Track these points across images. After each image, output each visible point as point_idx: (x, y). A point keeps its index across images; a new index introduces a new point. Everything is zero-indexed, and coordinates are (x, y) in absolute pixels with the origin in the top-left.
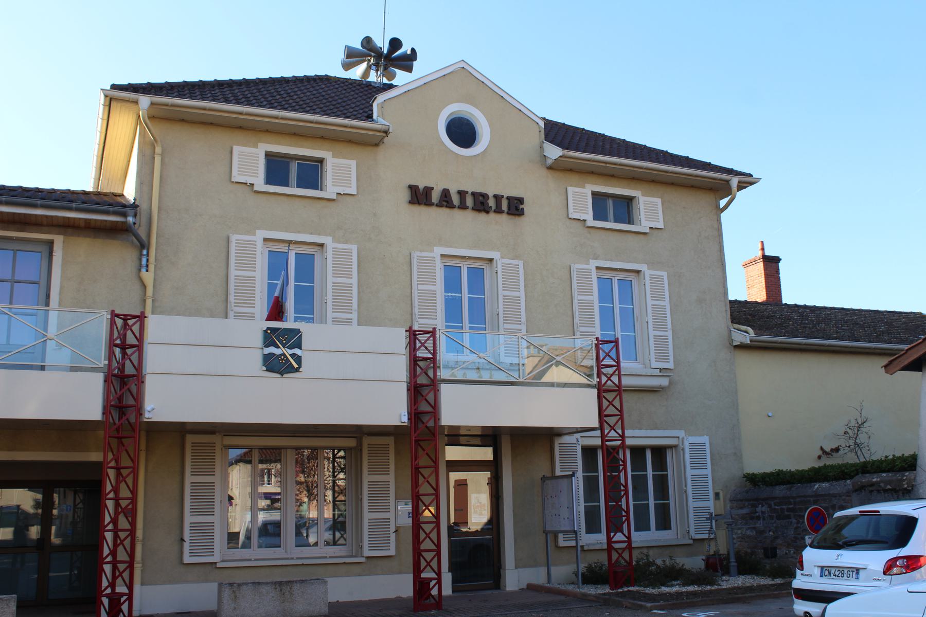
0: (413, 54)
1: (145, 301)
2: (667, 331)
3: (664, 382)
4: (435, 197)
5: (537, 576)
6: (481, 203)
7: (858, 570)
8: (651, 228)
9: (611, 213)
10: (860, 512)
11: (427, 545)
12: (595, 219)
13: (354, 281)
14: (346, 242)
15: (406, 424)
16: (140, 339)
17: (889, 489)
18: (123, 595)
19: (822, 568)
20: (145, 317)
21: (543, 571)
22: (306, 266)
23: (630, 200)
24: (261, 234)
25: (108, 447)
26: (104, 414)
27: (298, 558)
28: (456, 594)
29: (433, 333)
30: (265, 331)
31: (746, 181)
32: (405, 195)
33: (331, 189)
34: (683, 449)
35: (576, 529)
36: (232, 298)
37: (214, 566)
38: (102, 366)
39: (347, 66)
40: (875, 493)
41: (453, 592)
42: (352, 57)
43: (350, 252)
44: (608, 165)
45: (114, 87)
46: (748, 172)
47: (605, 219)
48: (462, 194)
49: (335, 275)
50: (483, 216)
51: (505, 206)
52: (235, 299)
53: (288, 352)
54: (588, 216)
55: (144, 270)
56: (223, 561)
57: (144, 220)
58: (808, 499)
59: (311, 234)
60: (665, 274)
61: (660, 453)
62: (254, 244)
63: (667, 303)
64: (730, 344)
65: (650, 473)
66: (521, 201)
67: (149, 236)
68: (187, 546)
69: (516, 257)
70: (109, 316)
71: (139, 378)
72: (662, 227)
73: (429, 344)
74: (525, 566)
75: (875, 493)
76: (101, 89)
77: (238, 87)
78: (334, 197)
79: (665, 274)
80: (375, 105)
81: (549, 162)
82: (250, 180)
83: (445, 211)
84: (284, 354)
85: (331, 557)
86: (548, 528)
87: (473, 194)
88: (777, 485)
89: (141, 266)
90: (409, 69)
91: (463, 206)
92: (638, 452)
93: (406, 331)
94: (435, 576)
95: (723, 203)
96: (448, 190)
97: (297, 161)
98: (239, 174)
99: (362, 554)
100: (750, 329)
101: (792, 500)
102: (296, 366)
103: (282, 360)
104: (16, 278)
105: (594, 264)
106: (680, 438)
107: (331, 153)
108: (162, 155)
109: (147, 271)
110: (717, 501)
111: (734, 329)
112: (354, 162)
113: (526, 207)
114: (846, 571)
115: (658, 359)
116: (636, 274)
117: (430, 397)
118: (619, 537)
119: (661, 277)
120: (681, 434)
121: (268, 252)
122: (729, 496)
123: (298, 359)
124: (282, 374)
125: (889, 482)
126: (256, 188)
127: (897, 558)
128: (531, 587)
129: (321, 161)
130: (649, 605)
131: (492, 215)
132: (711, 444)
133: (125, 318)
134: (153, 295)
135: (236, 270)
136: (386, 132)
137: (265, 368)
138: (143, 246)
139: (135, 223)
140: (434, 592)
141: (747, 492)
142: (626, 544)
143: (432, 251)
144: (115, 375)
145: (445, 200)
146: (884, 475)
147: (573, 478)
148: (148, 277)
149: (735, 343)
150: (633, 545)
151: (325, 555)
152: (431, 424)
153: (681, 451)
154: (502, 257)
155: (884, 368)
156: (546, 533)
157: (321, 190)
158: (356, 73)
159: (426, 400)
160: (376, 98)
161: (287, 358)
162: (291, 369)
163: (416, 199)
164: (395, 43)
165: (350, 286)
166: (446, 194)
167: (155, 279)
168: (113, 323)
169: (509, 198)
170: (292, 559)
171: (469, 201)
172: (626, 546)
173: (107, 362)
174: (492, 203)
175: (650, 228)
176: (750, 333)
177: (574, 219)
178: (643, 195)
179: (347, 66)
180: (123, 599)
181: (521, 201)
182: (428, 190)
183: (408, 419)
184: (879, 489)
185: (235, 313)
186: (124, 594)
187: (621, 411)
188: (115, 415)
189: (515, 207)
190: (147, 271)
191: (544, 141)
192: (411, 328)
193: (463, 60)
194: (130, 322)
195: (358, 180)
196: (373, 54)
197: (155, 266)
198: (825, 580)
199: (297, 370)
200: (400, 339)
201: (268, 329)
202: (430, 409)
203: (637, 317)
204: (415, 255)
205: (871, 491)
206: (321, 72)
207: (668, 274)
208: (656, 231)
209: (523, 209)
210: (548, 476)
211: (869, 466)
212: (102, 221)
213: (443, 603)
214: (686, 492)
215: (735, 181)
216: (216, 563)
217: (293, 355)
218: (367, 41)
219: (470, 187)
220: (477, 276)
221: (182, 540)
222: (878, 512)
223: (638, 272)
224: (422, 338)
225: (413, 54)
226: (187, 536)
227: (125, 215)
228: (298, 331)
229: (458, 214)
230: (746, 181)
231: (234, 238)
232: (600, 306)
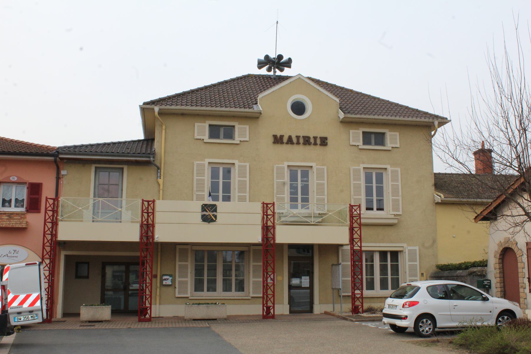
0: (290, 60)
1: (159, 191)
2: (399, 197)
3: (395, 221)
4: (285, 140)
5: (329, 308)
6: (307, 141)
7: (396, 306)
8: (393, 147)
9: (373, 141)
10: (407, 284)
11: (269, 292)
12: (364, 144)
13: (247, 179)
14: (244, 162)
15: (261, 242)
16: (153, 210)
17: (479, 275)
18: (148, 307)
19: (389, 305)
20: (155, 201)
21: (331, 306)
22: (228, 173)
23: (383, 134)
24: (207, 161)
25: (142, 251)
26: (140, 239)
27: (223, 296)
28: (291, 314)
29: (273, 204)
30: (202, 206)
31: (443, 121)
32: (272, 140)
33: (237, 139)
34: (405, 252)
35: (340, 288)
36: (195, 189)
37: (188, 298)
38: (139, 220)
39: (260, 67)
40: (475, 276)
41: (290, 313)
42: (261, 64)
43: (245, 166)
44: (368, 120)
45: (145, 104)
46: (445, 116)
47: (369, 143)
48: (298, 137)
49: (239, 177)
50: (307, 147)
51: (318, 141)
52: (196, 189)
53: (211, 214)
54: (360, 143)
55: (159, 178)
56: (192, 296)
57: (158, 157)
58: (454, 278)
59: (229, 159)
60: (399, 169)
61: (395, 255)
62: (204, 165)
63: (399, 183)
64: (433, 202)
65: (389, 263)
66: (326, 138)
67: (161, 164)
68: (177, 290)
69: (323, 165)
70: (141, 201)
71: (153, 226)
72: (399, 146)
73: (272, 208)
74: (324, 303)
75: (475, 276)
76: (139, 105)
77: (201, 91)
78: (239, 142)
79: (399, 169)
80: (258, 98)
81: (341, 120)
82: (202, 137)
83: (289, 146)
84: (210, 215)
85: (236, 296)
86: (334, 287)
87: (303, 137)
88: (446, 270)
89: (158, 176)
90: (290, 67)
91: (298, 143)
92: (383, 254)
93: (262, 203)
94: (272, 305)
95: (433, 133)
96: (291, 136)
97: (223, 127)
98: (197, 135)
99: (250, 296)
100: (442, 195)
101: (449, 278)
102: (214, 219)
103: (209, 217)
104: (111, 183)
105: (362, 166)
106: (404, 247)
107: (238, 123)
108: (166, 129)
109: (160, 178)
110: (422, 277)
111: (436, 194)
112: (248, 126)
113: (329, 141)
114: (394, 306)
115: (393, 210)
116: (384, 170)
117: (272, 231)
118: (357, 292)
119: (397, 171)
120: (405, 245)
121: (211, 168)
122: (429, 275)
123: (215, 217)
124: (209, 222)
125: (479, 272)
126: (205, 141)
127: (407, 302)
128: (326, 313)
129: (234, 126)
130: (354, 320)
131: (312, 147)
132: (419, 250)
133: (148, 202)
134: (163, 188)
135: (197, 176)
136: (261, 113)
137: (202, 220)
138: (159, 168)
139: (154, 161)
140: (272, 311)
141: (435, 273)
142: (360, 295)
143: (283, 164)
144: (144, 224)
145: (290, 141)
146: (479, 268)
147: (340, 265)
148: (161, 181)
149: (436, 202)
150: (364, 296)
151: (234, 295)
152: (272, 242)
153: (404, 254)
154: (317, 165)
155: (474, 220)
156: (333, 289)
157: (234, 140)
158: (264, 71)
159: (271, 232)
160: (258, 96)
161: (211, 216)
162: (212, 221)
163: (276, 141)
164: (280, 57)
165: (246, 181)
166: (290, 138)
167: (163, 182)
168: (143, 203)
169: (321, 138)
170: (220, 296)
171: (301, 141)
172: (361, 296)
173: (141, 219)
174: (312, 141)
175: (392, 147)
176: (442, 197)
177: (353, 145)
178: (389, 131)
179: (260, 67)
180: (148, 309)
181: (326, 138)
182: (282, 137)
183: (262, 240)
184: (476, 274)
185: (196, 194)
186: (149, 307)
187: (360, 236)
188: (145, 239)
189: (324, 142)
190: (160, 178)
191: (339, 109)
192: (263, 202)
193: (299, 74)
194: (150, 203)
195: (249, 134)
196: (271, 62)
197: (163, 176)
198: (389, 310)
199: (215, 221)
200: (258, 208)
201: (203, 204)
202: (272, 236)
203: (385, 191)
204: (275, 167)
205: (474, 275)
206: (245, 73)
207: (401, 169)
208: (396, 149)
209: (327, 143)
210: (335, 264)
211: (476, 263)
212: (141, 160)
213: (275, 316)
214: (406, 272)
215: (436, 123)
216: (188, 297)
217: (213, 215)
218: (267, 57)
219: (302, 134)
220: (305, 174)
221: (175, 288)
222: (411, 284)
223: (386, 169)
224: (269, 206)
225: (290, 60)
226: (177, 286)
227: (150, 157)
228: (215, 205)
229: (295, 147)
230: (443, 121)
231: (196, 163)
232: (366, 185)
